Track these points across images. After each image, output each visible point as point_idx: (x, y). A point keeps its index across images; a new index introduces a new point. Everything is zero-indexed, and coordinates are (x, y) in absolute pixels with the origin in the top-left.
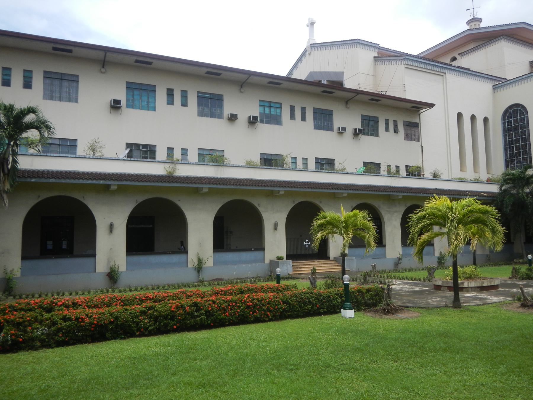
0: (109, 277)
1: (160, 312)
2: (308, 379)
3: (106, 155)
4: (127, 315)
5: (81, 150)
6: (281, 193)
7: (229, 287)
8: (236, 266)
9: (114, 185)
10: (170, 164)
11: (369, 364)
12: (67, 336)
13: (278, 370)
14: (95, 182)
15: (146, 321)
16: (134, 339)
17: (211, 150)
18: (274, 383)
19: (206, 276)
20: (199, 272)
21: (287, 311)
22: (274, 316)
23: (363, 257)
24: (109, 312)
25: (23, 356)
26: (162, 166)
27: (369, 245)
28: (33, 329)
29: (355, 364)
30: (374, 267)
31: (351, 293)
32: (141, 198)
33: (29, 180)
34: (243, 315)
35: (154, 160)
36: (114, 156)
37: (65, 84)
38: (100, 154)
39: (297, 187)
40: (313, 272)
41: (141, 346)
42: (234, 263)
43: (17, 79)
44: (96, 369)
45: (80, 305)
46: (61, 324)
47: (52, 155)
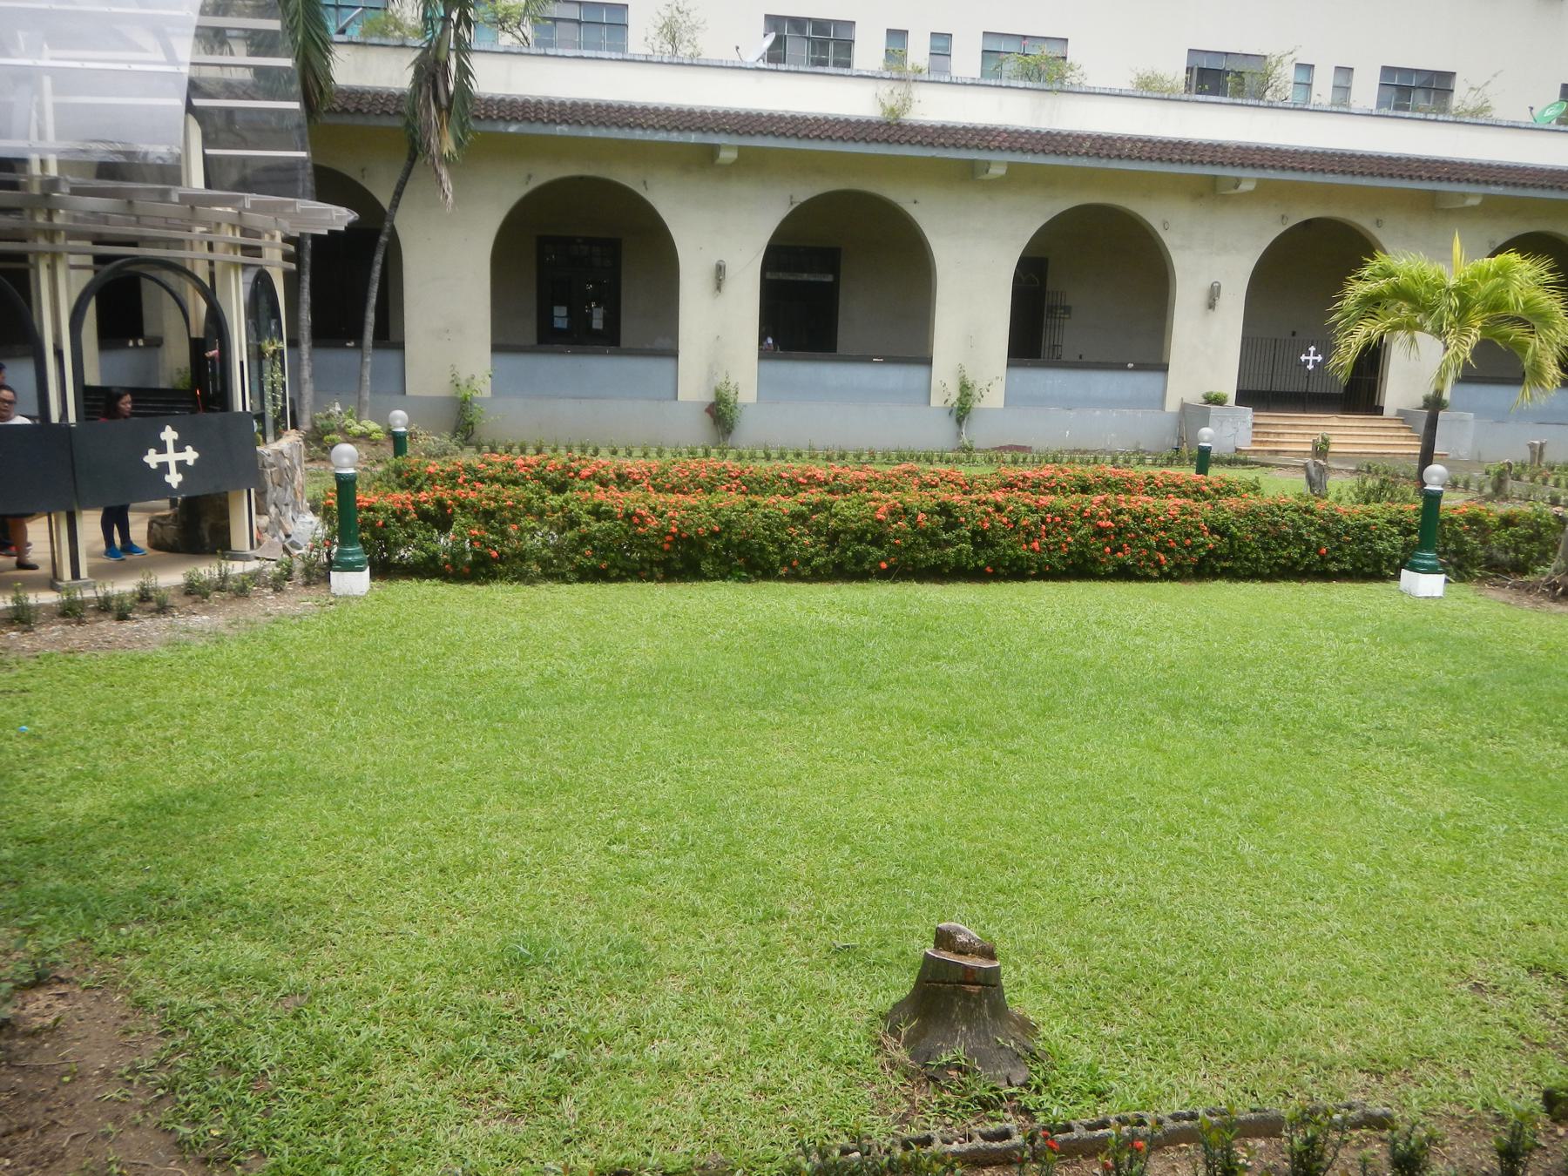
0: (712, 415)
1: (844, 521)
2: (1266, 754)
3: (710, 53)
4: (755, 520)
6: (1246, 187)
7: (1048, 470)
8: (1072, 413)
9: (730, 147)
10: (893, 84)
11: (1474, 738)
12: (604, 558)
13: (1175, 717)
14: (675, 137)
15: (807, 540)
16: (771, 584)
17: (1025, 37)
18: (1158, 750)
19: (980, 433)
20: (960, 421)
21: (1219, 558)
22: (1178, 566)
23: (1501, 417)
24: (710, 506)
25: (499, 594)
26: (869, 88)
27: (1538, 372)
28: (522, 530)
29: (1425, 732)
30: (1538, 452)
31: (1443, 522)
32: (805, 192)
33: (501, 127)
34: (1082, 554)
35: (845, 71)
36: (731, 57)
38: (690, 50)
39: (1303, 169)
40: (1321, 450)
41: (791, 604)
42: (1069, 404)
44: (675, 647)
45: (635, 482)
46: (588, 524)
47: (560, 52)
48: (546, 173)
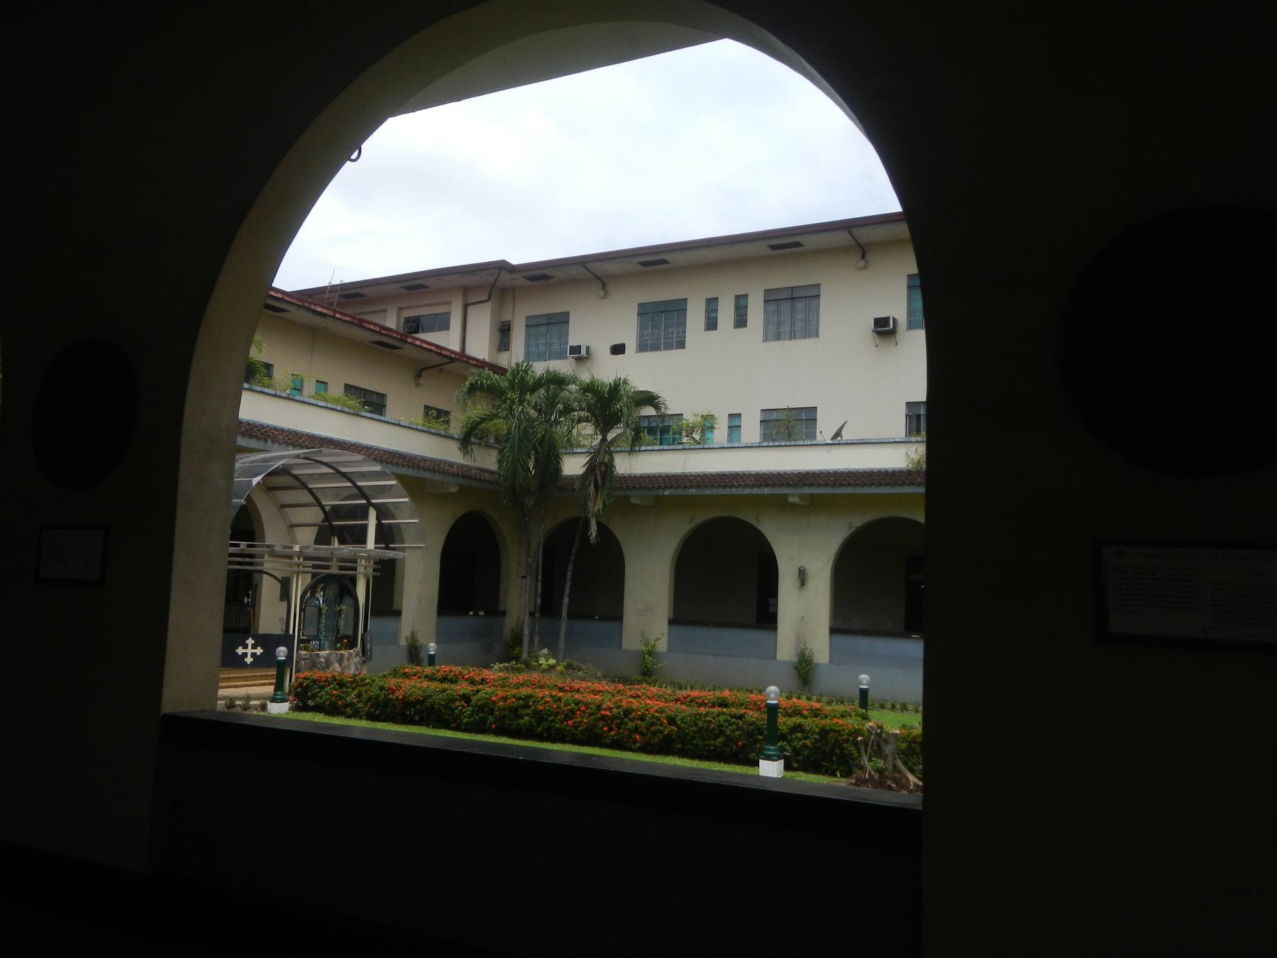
5: (825, 428)
9: (793, 495)
10: (916, 445)
14: (756, 491)
32: (859, 520)
33: (661, 492)
37: (800, 305)
43: (726, 314)
48: (702, 516)
